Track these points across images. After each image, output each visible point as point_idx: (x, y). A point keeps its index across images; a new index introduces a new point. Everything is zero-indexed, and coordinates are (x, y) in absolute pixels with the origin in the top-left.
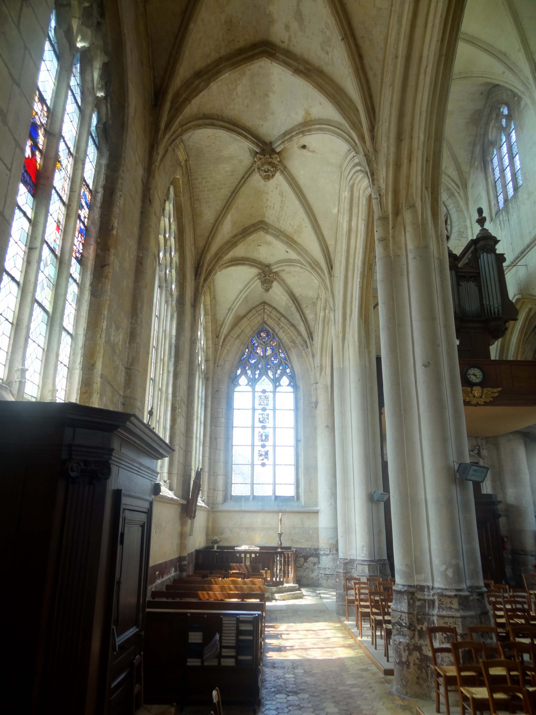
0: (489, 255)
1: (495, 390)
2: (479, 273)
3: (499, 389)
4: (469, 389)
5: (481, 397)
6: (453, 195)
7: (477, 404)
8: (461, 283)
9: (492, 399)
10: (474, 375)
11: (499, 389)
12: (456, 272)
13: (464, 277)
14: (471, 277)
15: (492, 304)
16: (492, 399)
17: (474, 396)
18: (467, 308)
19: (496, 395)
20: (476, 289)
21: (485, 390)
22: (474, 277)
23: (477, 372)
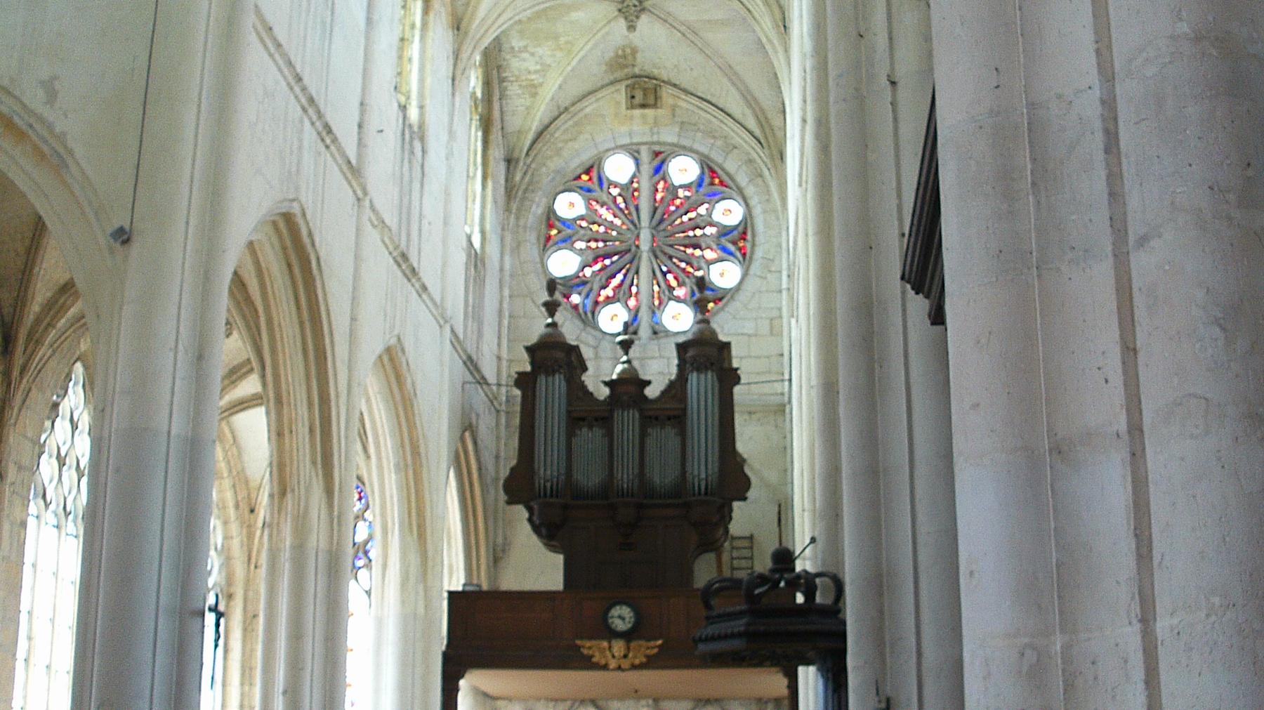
0: (702, 376)
1: (652, 643)
2: (685, 410)
3: (660, 642)
4: (605, 644)
5: (625, 656)
6: (761, 176)
7: (619, 668)
8: (649, 430)
9: (644, 660)
10: (620, 617)
11: (660, 642)
12: (641, 411)
13: (657, 418)
14: (669, 419)
15: (696, 472)
16: (644, 660)
17: (613, 657)
18: (657, 480)
19: (656, 650)
20: (678, 440)
21: (633, 644)
22: (675, 417)
23: (625, 611)
